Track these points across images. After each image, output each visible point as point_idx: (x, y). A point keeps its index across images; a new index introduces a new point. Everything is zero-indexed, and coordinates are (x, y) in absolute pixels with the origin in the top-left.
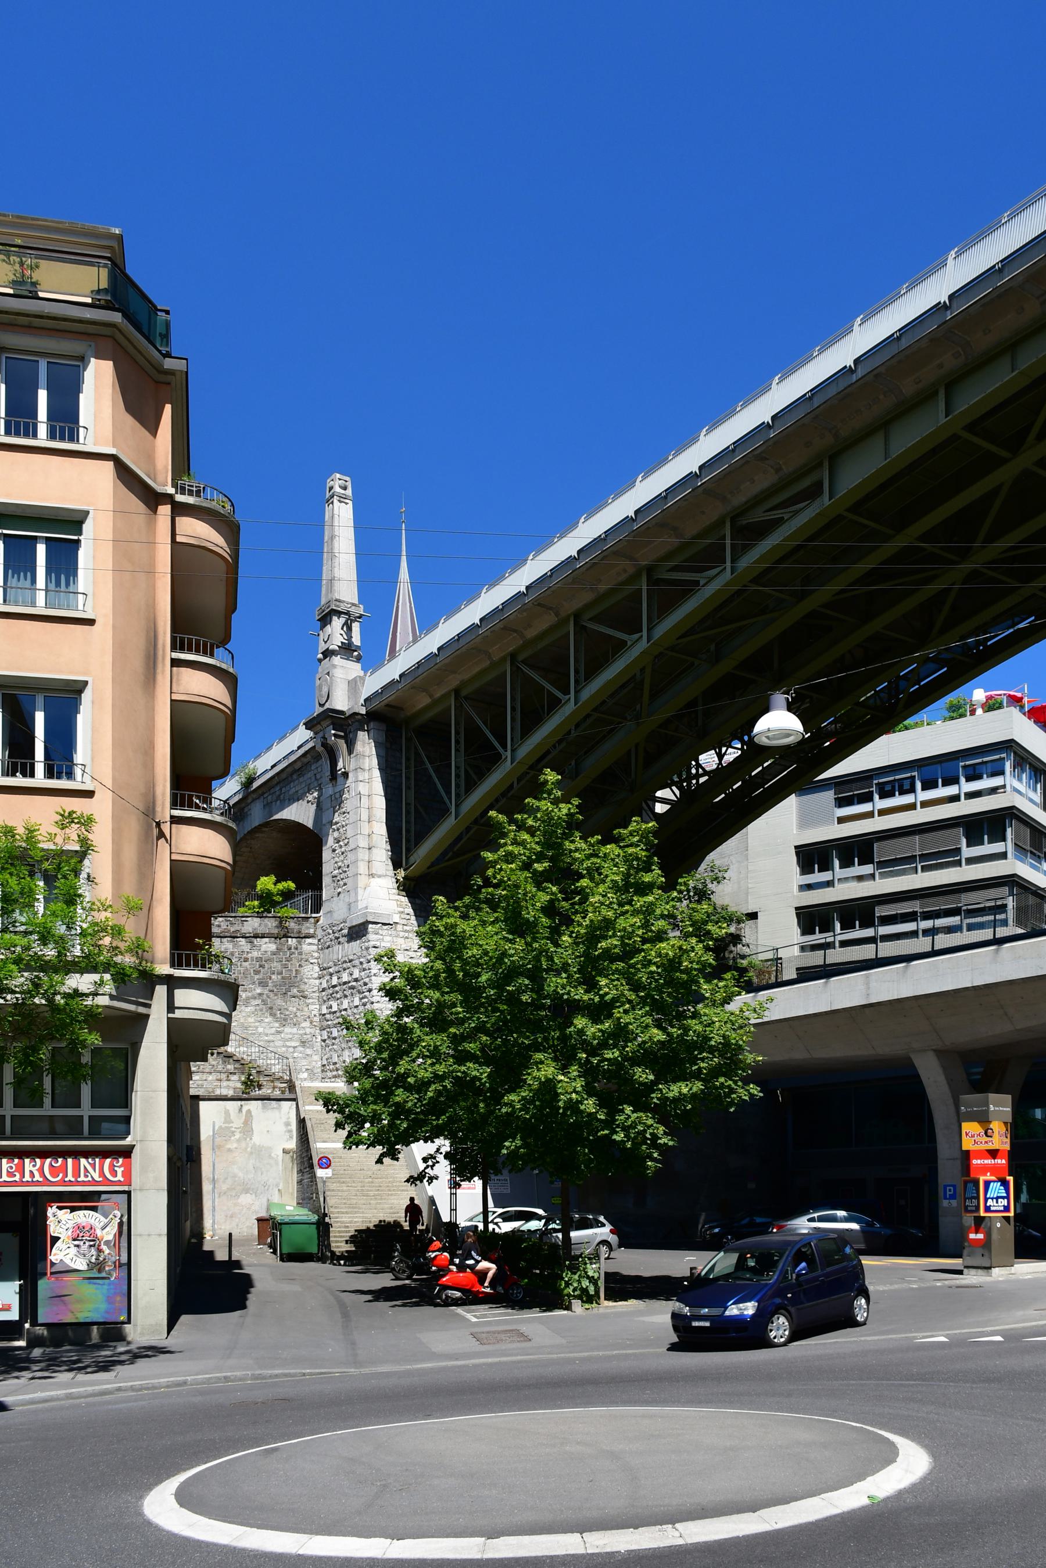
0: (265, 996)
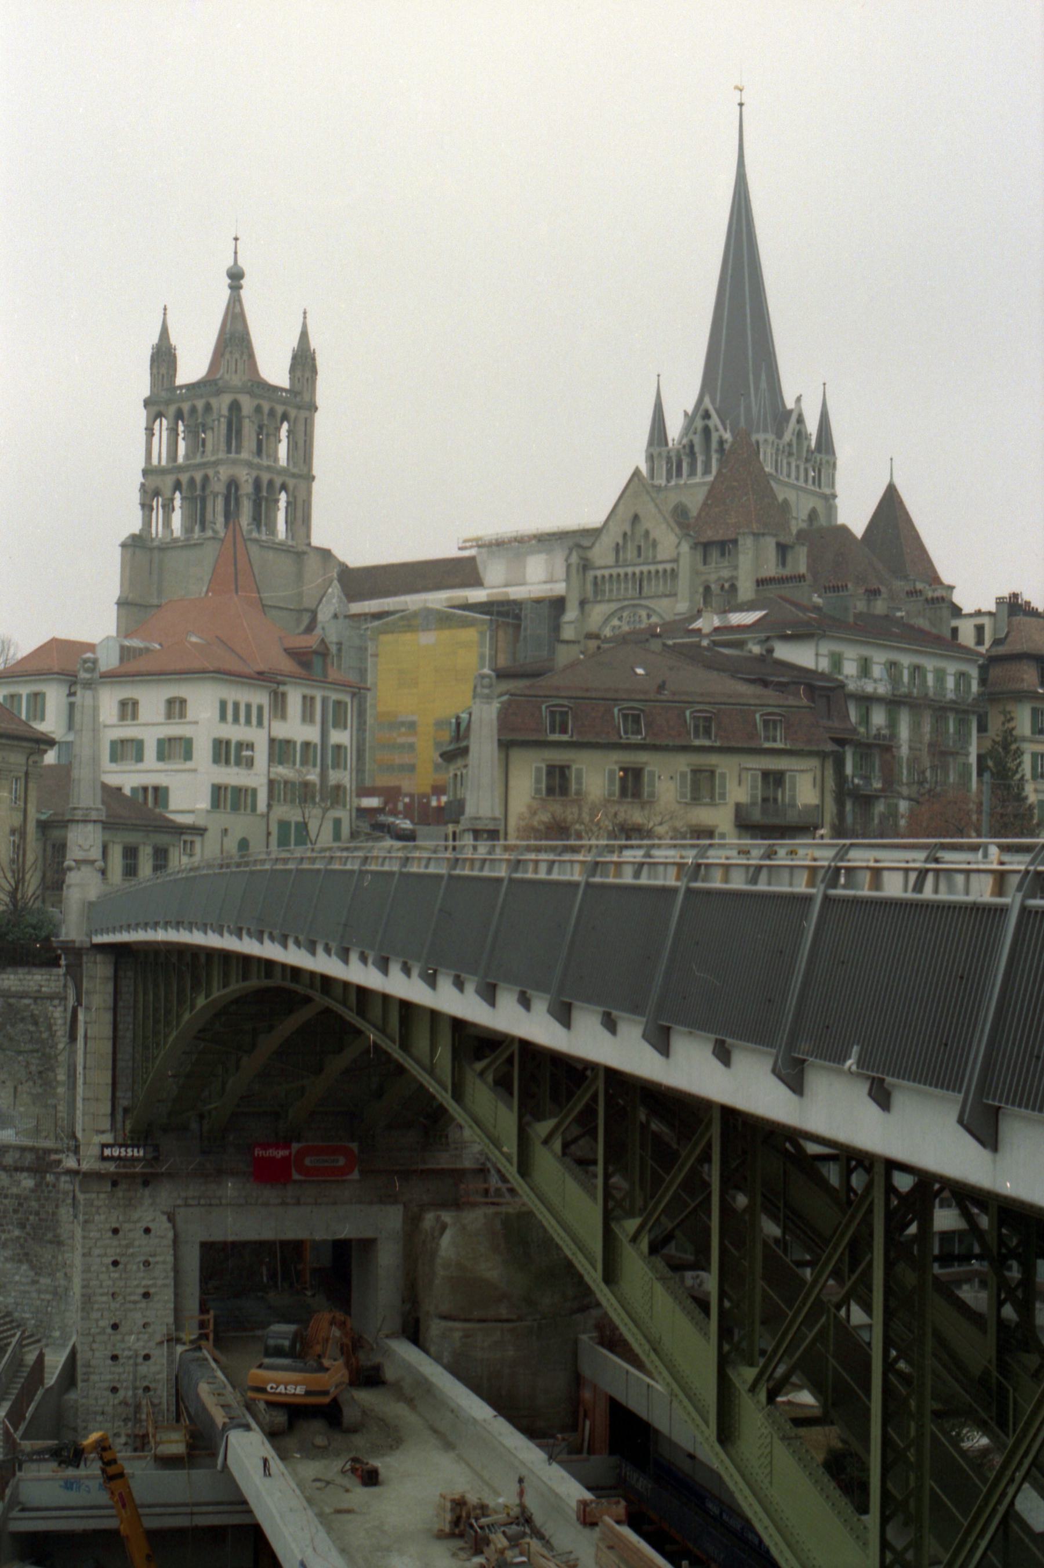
0: (22, 1240)
